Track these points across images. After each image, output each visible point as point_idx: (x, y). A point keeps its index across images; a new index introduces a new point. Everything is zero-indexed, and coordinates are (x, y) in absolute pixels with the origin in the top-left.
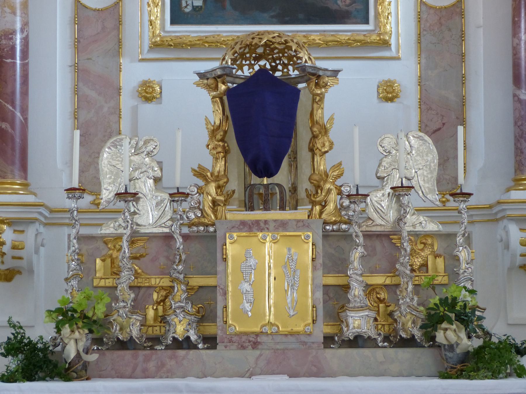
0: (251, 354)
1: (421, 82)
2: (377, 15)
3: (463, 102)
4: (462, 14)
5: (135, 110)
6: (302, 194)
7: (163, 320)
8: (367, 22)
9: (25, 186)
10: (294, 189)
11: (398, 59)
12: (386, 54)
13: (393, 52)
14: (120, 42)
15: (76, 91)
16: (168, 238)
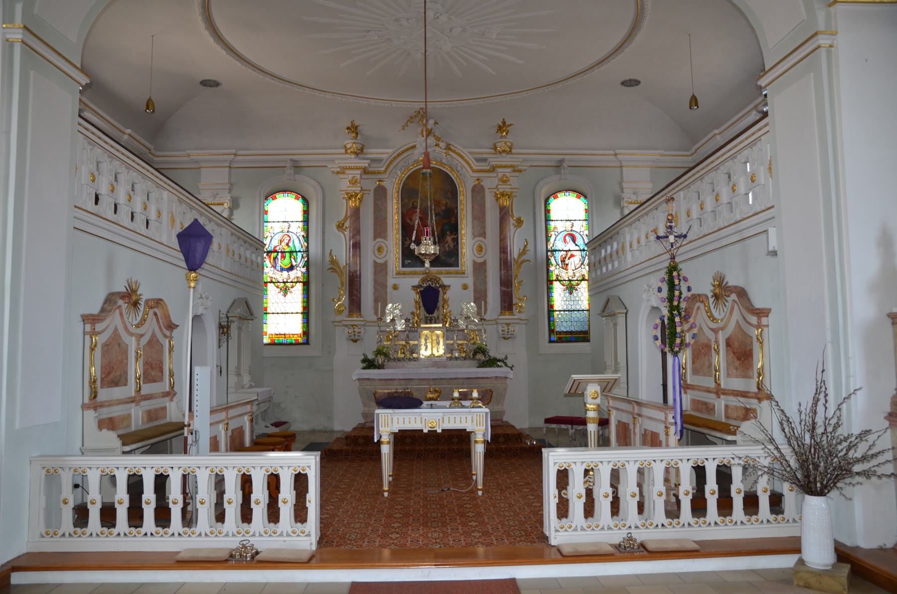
1: (474, 283)
3: (486, 290)
8: (458, 267)
9: (360, 315)
10: (438, 317)
11: (467, 277)
12: (464, 276)
13: (466, 275)
15: (375, 287)
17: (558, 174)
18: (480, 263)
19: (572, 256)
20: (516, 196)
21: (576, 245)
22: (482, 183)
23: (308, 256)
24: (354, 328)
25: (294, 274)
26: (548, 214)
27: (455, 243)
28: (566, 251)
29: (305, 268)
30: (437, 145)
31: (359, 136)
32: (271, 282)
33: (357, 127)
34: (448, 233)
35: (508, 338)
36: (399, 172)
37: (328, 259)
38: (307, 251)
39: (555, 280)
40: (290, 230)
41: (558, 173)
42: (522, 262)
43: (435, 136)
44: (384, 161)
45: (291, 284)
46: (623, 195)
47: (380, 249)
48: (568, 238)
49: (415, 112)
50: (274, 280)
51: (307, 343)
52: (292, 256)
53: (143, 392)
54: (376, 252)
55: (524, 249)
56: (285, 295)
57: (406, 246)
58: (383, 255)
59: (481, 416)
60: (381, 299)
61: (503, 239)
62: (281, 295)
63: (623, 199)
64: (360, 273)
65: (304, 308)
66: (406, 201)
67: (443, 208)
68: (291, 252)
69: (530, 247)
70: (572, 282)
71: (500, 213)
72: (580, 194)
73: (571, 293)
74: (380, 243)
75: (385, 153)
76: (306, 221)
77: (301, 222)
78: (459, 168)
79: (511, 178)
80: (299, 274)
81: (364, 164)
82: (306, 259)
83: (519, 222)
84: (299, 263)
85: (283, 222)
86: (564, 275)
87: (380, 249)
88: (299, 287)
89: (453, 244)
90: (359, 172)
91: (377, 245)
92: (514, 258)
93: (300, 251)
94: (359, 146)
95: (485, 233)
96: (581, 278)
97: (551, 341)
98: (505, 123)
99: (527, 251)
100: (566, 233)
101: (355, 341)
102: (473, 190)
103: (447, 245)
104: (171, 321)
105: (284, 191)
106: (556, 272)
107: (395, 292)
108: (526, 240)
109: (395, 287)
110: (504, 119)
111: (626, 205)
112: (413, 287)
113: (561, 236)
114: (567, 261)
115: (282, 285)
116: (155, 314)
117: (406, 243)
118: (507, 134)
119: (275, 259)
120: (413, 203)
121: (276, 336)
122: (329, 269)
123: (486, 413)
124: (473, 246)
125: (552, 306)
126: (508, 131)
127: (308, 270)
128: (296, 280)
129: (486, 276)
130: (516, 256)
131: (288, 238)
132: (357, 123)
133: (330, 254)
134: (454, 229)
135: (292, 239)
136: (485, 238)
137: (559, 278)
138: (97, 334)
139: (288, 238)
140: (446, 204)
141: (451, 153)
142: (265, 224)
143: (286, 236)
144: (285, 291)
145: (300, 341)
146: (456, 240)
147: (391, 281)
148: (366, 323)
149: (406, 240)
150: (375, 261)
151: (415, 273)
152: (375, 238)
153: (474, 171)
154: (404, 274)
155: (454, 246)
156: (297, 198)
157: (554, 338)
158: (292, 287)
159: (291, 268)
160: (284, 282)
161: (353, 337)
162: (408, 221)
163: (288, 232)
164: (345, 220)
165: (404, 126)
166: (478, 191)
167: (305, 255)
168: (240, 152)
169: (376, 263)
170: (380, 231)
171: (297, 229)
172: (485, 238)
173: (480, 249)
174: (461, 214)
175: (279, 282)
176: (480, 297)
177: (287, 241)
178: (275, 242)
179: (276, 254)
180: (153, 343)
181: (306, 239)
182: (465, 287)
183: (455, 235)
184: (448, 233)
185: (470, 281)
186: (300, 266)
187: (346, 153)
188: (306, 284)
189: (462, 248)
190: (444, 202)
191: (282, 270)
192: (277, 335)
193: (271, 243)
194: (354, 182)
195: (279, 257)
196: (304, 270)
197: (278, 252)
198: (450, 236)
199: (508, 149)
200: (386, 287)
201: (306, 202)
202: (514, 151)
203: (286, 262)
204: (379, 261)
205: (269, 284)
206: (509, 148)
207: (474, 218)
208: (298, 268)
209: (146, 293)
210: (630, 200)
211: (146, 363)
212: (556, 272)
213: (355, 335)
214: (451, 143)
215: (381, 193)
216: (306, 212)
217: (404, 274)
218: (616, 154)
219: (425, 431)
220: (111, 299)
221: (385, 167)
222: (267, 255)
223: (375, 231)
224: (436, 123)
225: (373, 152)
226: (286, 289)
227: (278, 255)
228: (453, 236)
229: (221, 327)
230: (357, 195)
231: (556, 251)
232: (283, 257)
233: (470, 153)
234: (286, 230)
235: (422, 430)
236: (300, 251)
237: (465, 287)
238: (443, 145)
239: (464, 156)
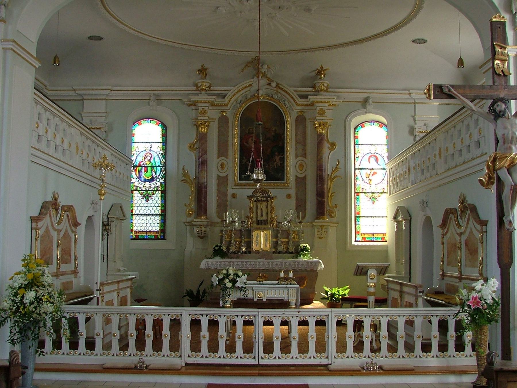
0: (258, 255)
2: (286, 179)
3: (305, 199)
4: (306, 179)
6: (269, 222)
7: (240, 248)
8: (284, 181)
9: (206, 218)
12: (288, 188)
15: (217, 195)
16: (241, 230)
17: (365, 108)
18: (302, 178)
19: (375, 173)
20: (331, 126)
21: (378, 164)
22: (304, 115)
23: (165, 170)
25: (153, 185)
26: (356, 140)
27: (282, 162)
28: (370, 169)
29: (163, 180)
30: (269, 84)
31: (207, 76)
32: (136, 190)
33: (206, 69)
35: (322, 238)
37: (181, 172)
38: (165, 166)
39: (361, 193)
40: (152, 149)
41: (364, 107)
42: (335, 177)
43: (267, 77)
45: (152, 192)
46: (416, 126)
47: (222, 166)
48: (373, 159)
49: (252, 59)
50: (138, 189)
51: (164, 238)
52: (153, 170)
53: (61, 270)
54: (220, 168)
55: (336, 167)
56: (147, 201)
57: (244, 163)
58: (224, 171)
59: (294, 290)
60: (223, 207)
61: (319, 159)
62: (144, 201)
63: (416, 129)
64: (207, 185)
65: (162, 211)
66: (244, 128)
67: (273, 134)
68: (152, 167)
69: (341, 166)
70: (374, 194)
71: (317, 140)
72: (382, 124)
73: (373, 203)
76: (164, 142)
77: (161, 143)
78: (286, 103)
79: (326, 111)
80: (159, 184)
82: (164, 173)
83: (333, 145)
84: (159, 176)
85: (146, 143)
86: (368, 189)
87: (222, 166)
88: (158, 194)
89: (280, 162)
90: (207, 105)
91: (221, 162)
92: (328, 175)
93: (159, 166)
94: (208, 85)
95: (305, 154)
96: (382, 191)
97: (356, 241)
98: (323, 68)
99: (339, 168)
100: (370, 155)
101: (202, 238)
102: (297, 120)
103: (275, 163)
104: (77, 221)
105: (147, 118)
106: (362, 187)
108: (338, 160)
109: (234, 196)
110: (321, 66)
111: (417, 134)
112: (248, 196)
113: (367, 157)
114: (371, 178)
115: (145, 193)
116: (68, 216)
117: (243, 161)
118: (324, 76)
119: (139, 172)
120: (249, 130)
121: (140, 233)
122: (181, 181)
123: (297, 288)
124: (296, 164)
125: (358, 213)
126: (325, 74)
127: (165, 181)
128: (156, 189)
129: (306, 188)
130: (329, 173)
131: (150, 156)
132: (206, 66)
133: (183, 169)
134: (281, 150)
135: (153, 157)
136: (305, 157)
137: (364, 191)
138: (39, 229)
139: (150, 156)
140: (276, 130)
141: (279, 90)
142: (133, 144)
143: (149, 154)
144: (147, 197)
145: (159, 237)
146: (282, 160)
147: (230, 191)
148: (212, 224)
149: (243, 159)
150: (218, 175)
153: (297, 105)
154: (241, 185)
155: (281, 164)
156: (157, 124)
157: (359, 238)
158: (153, 194)
159: (152, 179)
160: (146, 190)
161: (200, 235)
162: (245, 144)
163: (150, 151)
166: (301, 120)
167: (163, 169)
168: (115, 88)
169: (219, 176)
170: (223, 151)
171: (157, 148)
172: (305, 157)
173: (301, 166)
174: (287, 139)
175: (142, 190)
176: (301, 206)
177: (149, 158)
178: (140, 159)
179: (140, 168)
180: (66, 236)
181: (164, 156)
182: (289, 196)
183: (282, 156)
184: (276, 153)
185: (293, 192)
186: (159, 178)
188: (164, 192)
189: (287, 166)
190: (274, 129)
191: (145, 180)
192: (141, 232)
193: (137, 158)
195: (143, 170)
196: (162, 181)
197: (142, 167)
198: (278, 156)
199: (325, 89)
200: (227, 195)
201: (164, 127)
202: (329, 90)
203: (149, 174)
205: (134, 192)
206: (326, 87)
207: (297, 142)
208: (158, 180)
209: (62, 201)
210: (421, 130)
211: (62, 250)
212: (362, 186)
213: (202, 233)
215: (223, 121)
216: (165, 136)
217: (241, 185)
218: (410, 94)
219: (255, 300)
220: (44, 207)
222: (133, 169)
224: (269, 68)
225: (219, 89)
226: (148, 195)
227: (142, 169)
228: (280, 156)
229: (104, 225)
230: (206, 123)
231: (362, 169)
232: (146, 171)
233: (296, 91)
234: (149, 149)
235: (253, 299)
236: (159, 166)
237: (289, 196)
238: (274, 84)
239: (291, 93)
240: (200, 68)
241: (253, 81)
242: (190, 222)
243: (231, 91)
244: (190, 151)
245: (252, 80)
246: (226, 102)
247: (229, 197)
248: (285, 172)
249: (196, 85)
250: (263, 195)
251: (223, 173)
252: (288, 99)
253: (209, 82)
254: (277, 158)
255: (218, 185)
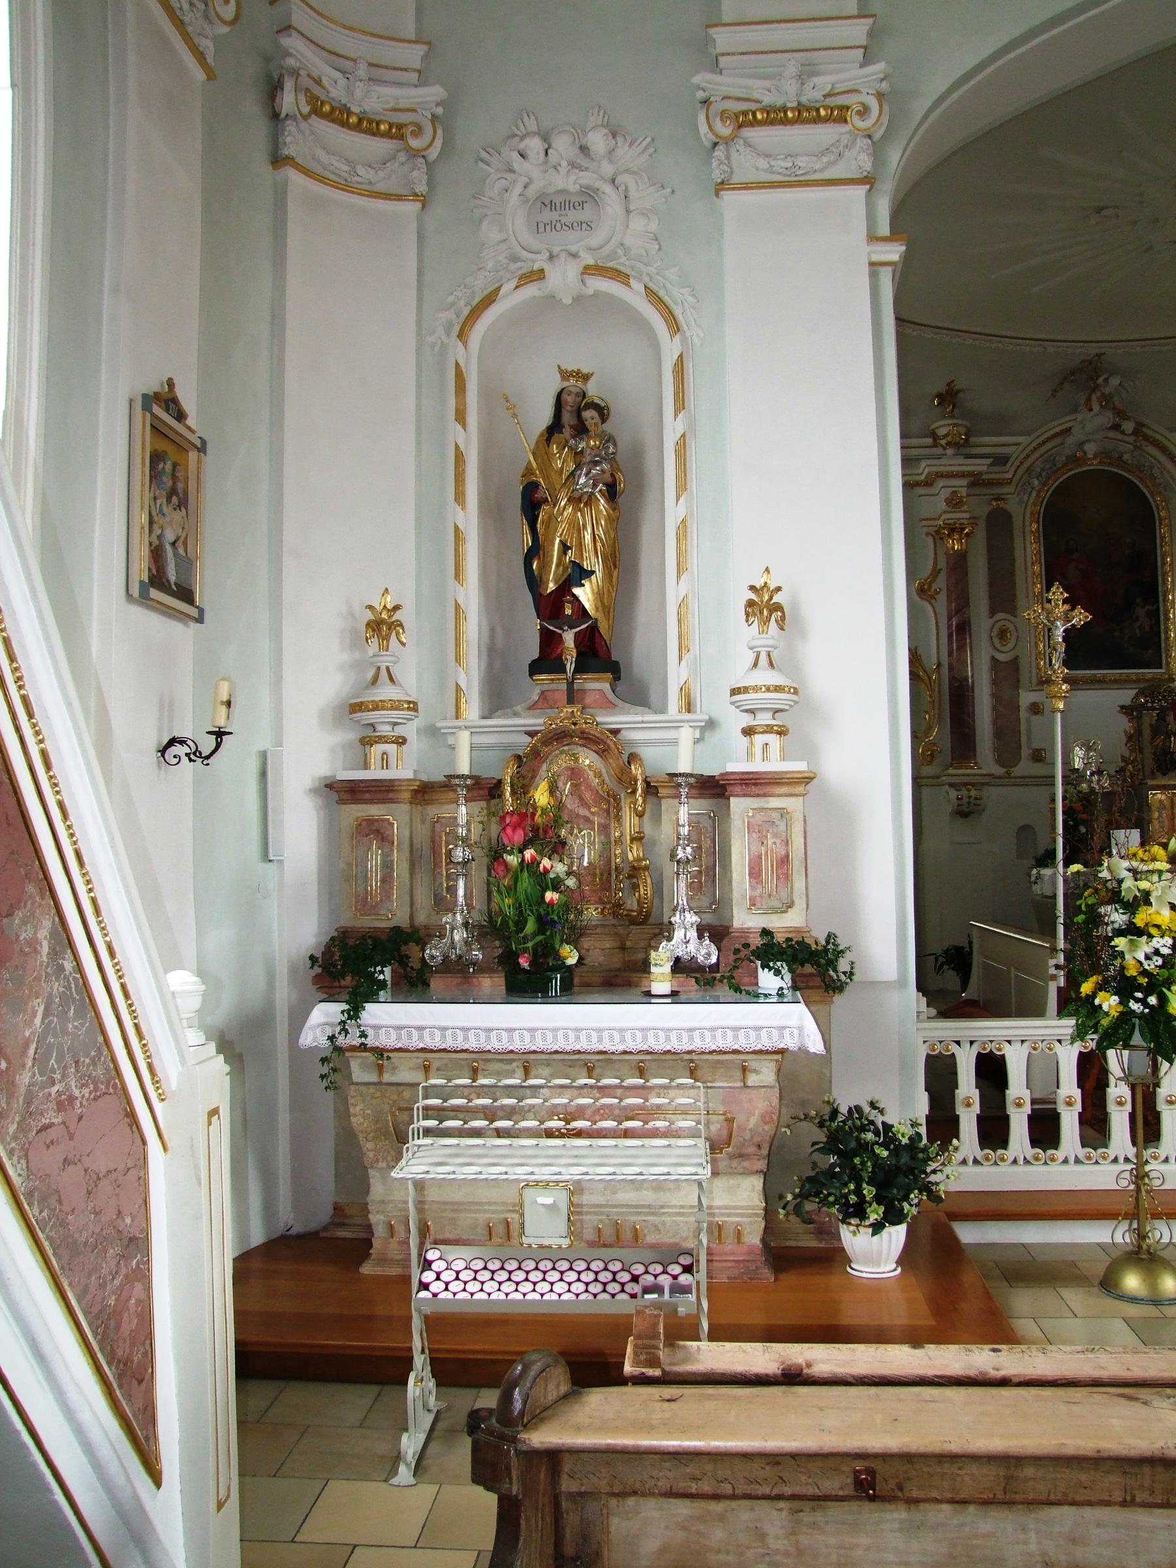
2: (1168, 664)
5: (1028, 721)
14: (1018, 681)
15: (994, 708)
24: (969, 790)
30: (1116, 427)
33: (958, 392)
34: (1138, 600)
36: (1036, 482)
44: (1010, 463)
47: (1003, 635)
49: (1083, 361)
54: (996, 641)
74: (1003, 623)
75: (1016, 444)
78: (1156, 472)
81: (980, 466)
87: (1003, 635)
90: (964, 482)
91: (998, 625)
103: (1137, 624)
107: (1035, 719)
112: (1122, 707)
132: (958, 385)
150: (993, 658)
151: (1118, 683)
152: (992, 613)
161: (965, 809)
164: (936, 572)
165: (1055, 391)
169: (997, 661)
174: (1164, 564)
187: (935, 445)
194: (954, 502)
200: (1018, 707)
204: (1001, 657)
214: (1147, 421)
221: (1013, 469)
223: (991, 598)
228: (1147, 607)
230: (964, 529)
238: (1129, 427)
240: (941, 387)
241: (1075, 420)
242: (938, 777)
243: (1021, 447)
244: (921, 598)
245: (1072, 417)
246: (1009, 476)
247: (1023, 714)
248: (1163, 645)
249: (933, 435)
250: (1153, 702)
251: (1003, 652)
252: (1159, 462)
253: (965, 423)
254: (1141, 612)
255: (995, 682)
